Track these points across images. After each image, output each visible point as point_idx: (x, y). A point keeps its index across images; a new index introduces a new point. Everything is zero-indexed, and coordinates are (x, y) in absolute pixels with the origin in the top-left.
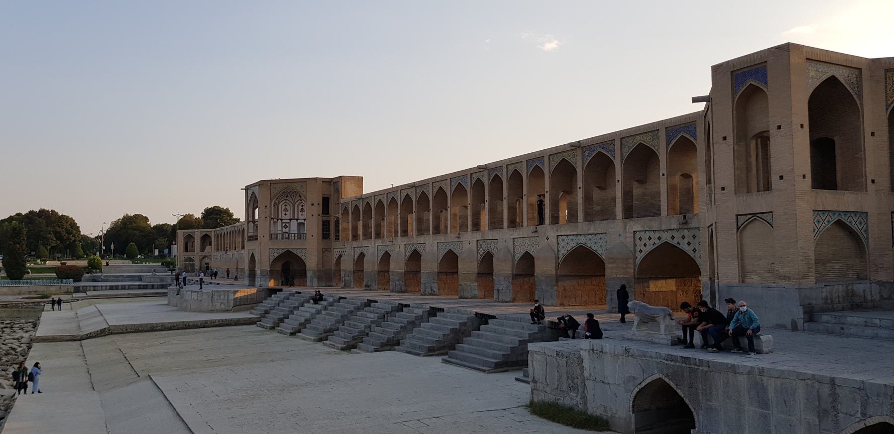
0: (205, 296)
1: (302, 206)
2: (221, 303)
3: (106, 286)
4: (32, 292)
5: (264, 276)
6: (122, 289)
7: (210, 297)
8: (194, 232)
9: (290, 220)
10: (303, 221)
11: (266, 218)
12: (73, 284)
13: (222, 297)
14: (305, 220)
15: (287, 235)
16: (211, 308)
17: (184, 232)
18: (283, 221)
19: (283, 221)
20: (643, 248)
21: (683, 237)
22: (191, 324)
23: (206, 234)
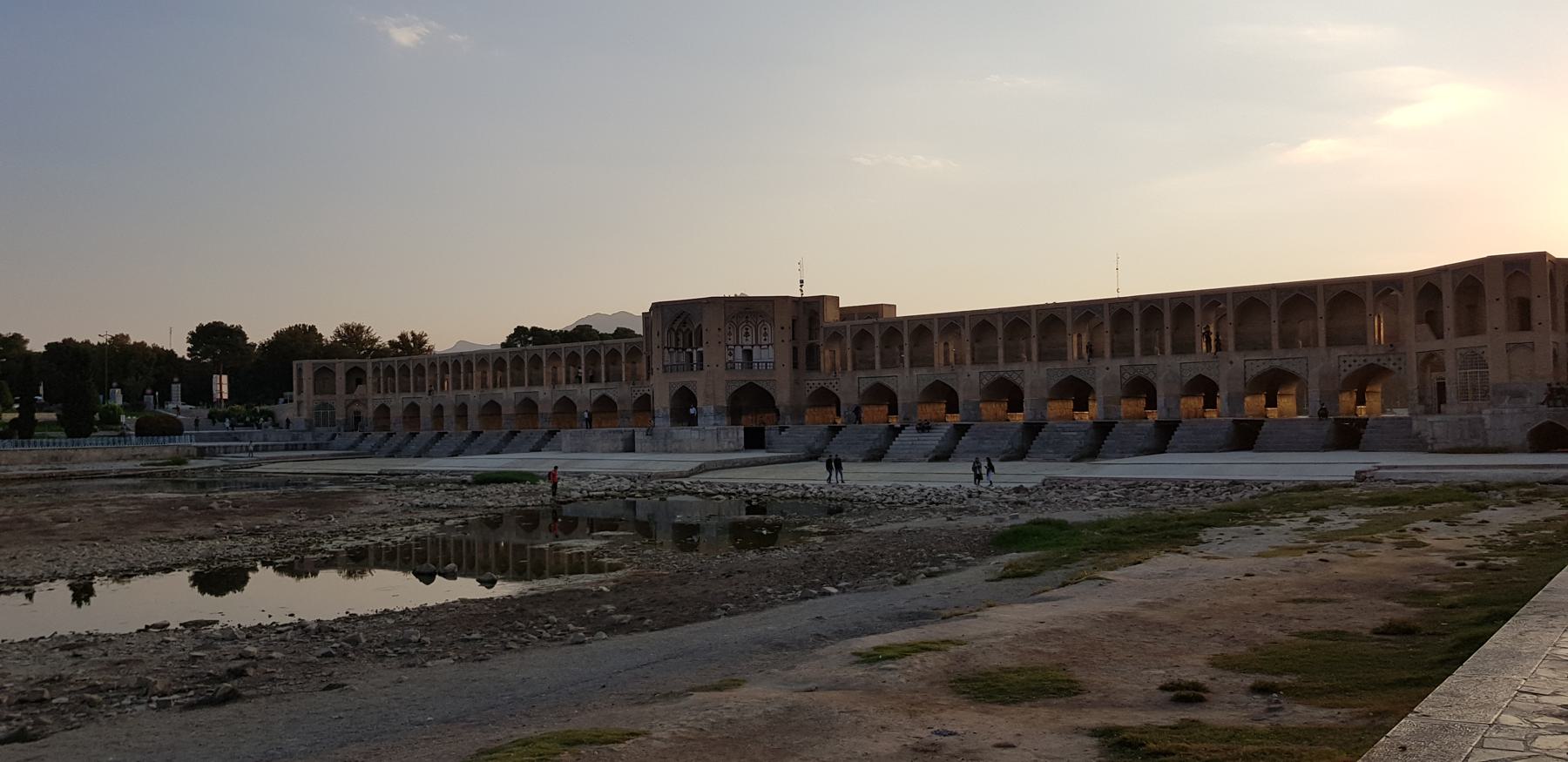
0: (709, 435)
1: (747, 329)
2: (730, 442)
3: (242, 446)
4: (139, 457)
5: (720, 413)
6: (263, 451)
7: (715, 436)
8: (334, 364)
9: (735, 346)
10: (750, 348)
11: (720, 343)
12: (195, 444)
13: (730, 435)
14: (753, 346)
15: (732, 365)
16: (716, 448)
17: (313, 364)
18: (730, 347)
19: (730, 347)
20: (1348, 368)
21: (1389, 360)
22: (760, 460)
23: (356, 367)
